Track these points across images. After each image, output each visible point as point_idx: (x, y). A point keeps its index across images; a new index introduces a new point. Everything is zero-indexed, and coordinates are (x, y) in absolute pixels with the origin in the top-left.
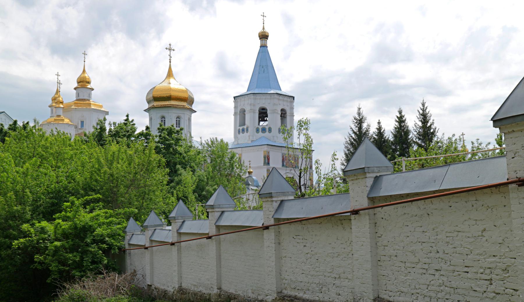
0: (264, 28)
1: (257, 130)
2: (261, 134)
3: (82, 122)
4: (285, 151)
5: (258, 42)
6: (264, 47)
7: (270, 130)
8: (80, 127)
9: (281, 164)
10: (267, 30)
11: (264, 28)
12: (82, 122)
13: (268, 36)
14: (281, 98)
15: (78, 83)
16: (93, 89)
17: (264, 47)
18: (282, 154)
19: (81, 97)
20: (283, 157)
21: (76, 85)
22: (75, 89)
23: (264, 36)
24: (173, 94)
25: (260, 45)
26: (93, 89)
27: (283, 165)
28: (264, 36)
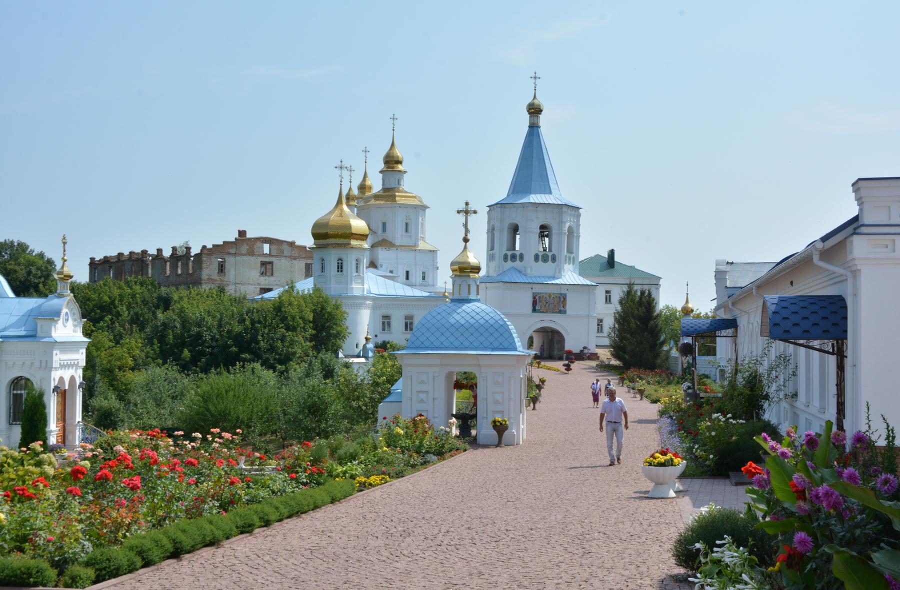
0: (535, 97)
1: (505, 258)
2: (510, 263)
3: (384, 224)
4: (537, 289)
6: (534, 128)
7: (522, 257)
10: (541, 101)
11: (535, 97)
12: (384, 224)
13: (541, 111)
16: (405, 172)
17: (534, 128)
18: (533, 293)
19: (388, 186)
20: (534, 298)
21: (381, 166)
22: (381, 172)
23: (534, 110)
24: (331, 232)
25: (528, 124)
26: (405, 172)
27: (534, 310)
28: (534, 110)
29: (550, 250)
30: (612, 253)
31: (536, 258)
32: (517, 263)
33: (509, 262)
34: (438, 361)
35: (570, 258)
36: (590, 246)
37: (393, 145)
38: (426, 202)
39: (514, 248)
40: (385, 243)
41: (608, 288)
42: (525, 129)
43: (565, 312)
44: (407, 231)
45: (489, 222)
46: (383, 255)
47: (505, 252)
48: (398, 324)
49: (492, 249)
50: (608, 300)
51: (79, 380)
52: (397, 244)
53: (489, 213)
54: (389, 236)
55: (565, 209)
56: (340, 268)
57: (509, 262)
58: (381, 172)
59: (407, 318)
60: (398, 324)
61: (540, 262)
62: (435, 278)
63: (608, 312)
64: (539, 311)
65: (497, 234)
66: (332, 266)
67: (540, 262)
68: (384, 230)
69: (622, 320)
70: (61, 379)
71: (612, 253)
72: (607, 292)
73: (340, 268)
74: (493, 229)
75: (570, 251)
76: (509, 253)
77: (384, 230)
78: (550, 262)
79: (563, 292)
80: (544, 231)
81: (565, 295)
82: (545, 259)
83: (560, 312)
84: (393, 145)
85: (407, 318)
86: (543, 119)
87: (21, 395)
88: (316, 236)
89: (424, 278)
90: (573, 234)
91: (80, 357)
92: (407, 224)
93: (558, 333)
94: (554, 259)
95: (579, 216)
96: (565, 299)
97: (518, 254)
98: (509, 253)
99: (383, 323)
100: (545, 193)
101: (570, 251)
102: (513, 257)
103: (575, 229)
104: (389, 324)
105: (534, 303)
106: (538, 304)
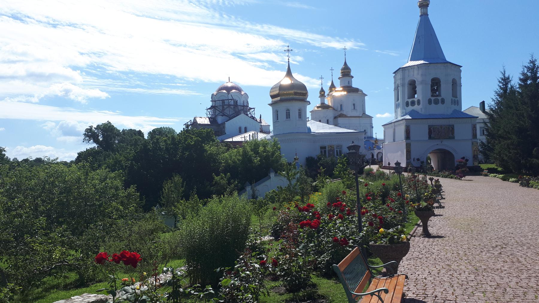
1: (407, 104)
2: (410, 108)
3: (341, 105)
5: (418, 12)
8: (339, 109)
12: (341, 105)
16: (353, 77)
17: (424, 16)
18: (429, 126)
20: (430, 129)
21: (340, 75)
22: (339, 78)
26: (353, 77)
27: (430, 138)
29: (439, 95)
31: (430, 102)
32: (416, 107)
33: (410, 106)
35: (455, 102)
37: (345, 63)
40: (341, 116)
42: (417, 19)
43: (453, 138)
45: (395, 83)
47: (406, 100)
49: (398, 100)
54: (344, 113)
56: (288, 116)
57: (410, 106)
58: (339, 78)
61: (433, 104)
62: (372, 132)
64: (434, 139)
65: (400, 89)
66: (282, 115)
67: (433, 104)
73: (288, 116)
74: (398, 87)
76: (410, 100)
78: (440, 104)
80: (435, 84)
81: (453, 126)
82: (436, 102)
84: (345, 63)
86: (430, 10)
88: (273, 97)
90: (456, 85)
94: (443, 101)
95: (461, 71)
97: (416, 100)
98: (410, 100)
99: (321, 152)
102: (413, 103)
103: (457, 80)
105: (430, 132)
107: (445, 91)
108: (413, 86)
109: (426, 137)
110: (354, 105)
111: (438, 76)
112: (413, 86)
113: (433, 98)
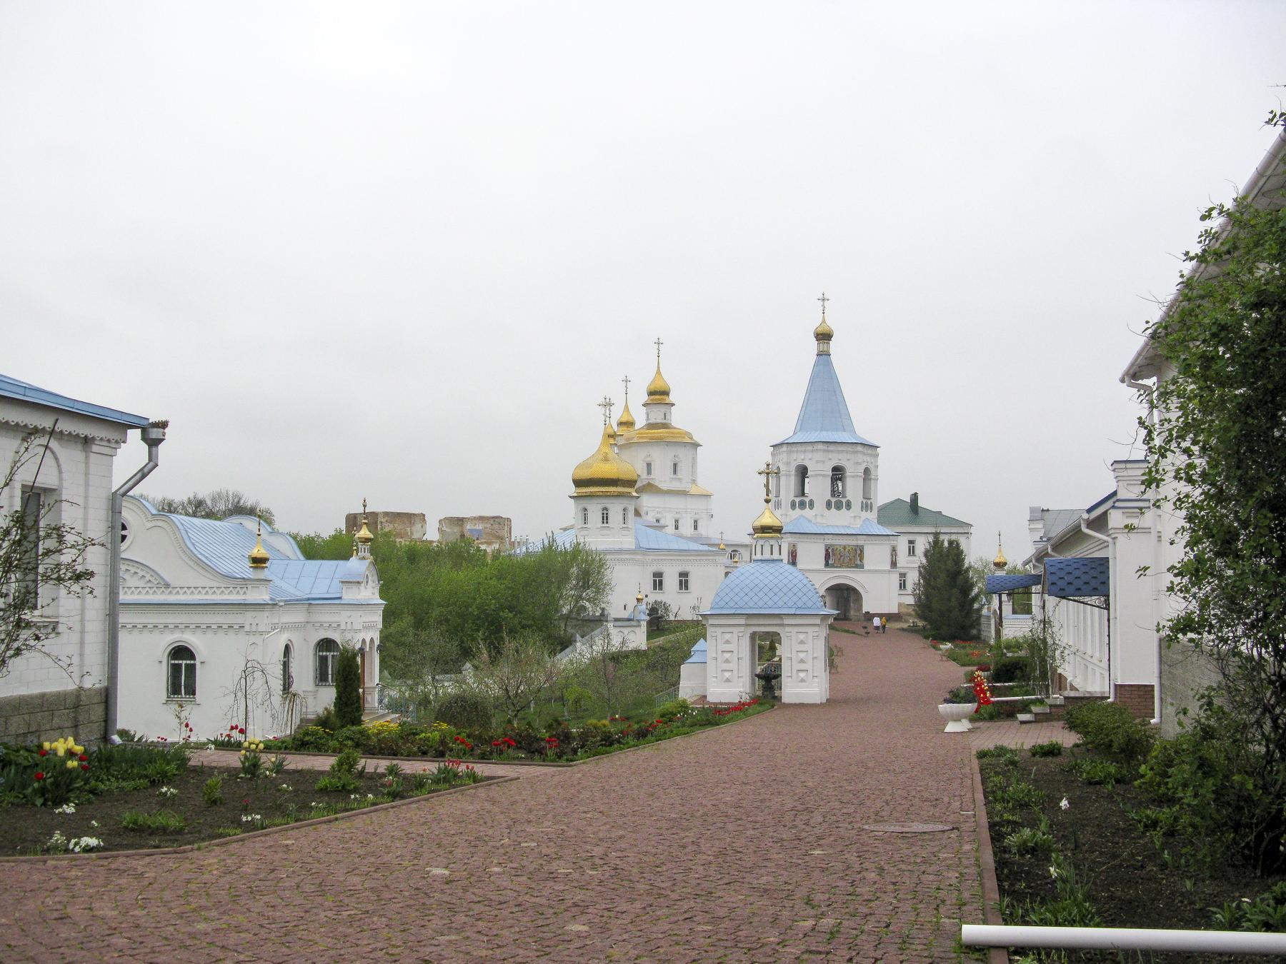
1: (793, 505)
3: (649, 465)
4: (830, 541)
6: (823, 355)
7: (812, 504)
9: (823, 562)
10: (833, 324)
12: (649, 465)
14: (832, 448)
15: (651, 393)
17: (823, 355)
19: (652, 421)
21: (645, 398)
23: (824, 337)
27: (827, 565)
28: (824, 337)
29: (844, 497)
30: (915, 497)
31: (829, 505)
34: (742, 621)
36: (889, 490)
37: (658, 372)
38: (697, 438)
39: (803, 494)
40: (650, 488)
41: (911, 537)
44: (675, 472)
46: (647, 502)
48: (671, 581)
50: (912, 552)
51: (377, 642)
52: (664, 486)
53: (773, 455)
55: (860, 448)
56: (605, 518)
59: (681, 575)
60: (671, 581)
63: (912, 565)
64: (833, 566)
68: (649, 472)
69: (928, 574)
70: (364, 641)
71: (915, 497)
72: (911, 542)
73: (605, 518)
75: (866, 496)
76: (797, 500)
77: (649, 472)
79: (860, 543)
83: (857, 566)
84: (658, 372)
85: (681, 575)
87: (326, 657)
89: (696, 528)
91: (377, 618)
92: (675, 465)
93: (854, 590)
94: (849, 506)
96: (862, 551)
97: (807, 500)
98: (797, 500)
100: (837, 430)
101: (866, 496)
102: (802, 505)
104: (661, 582)
106: (832, 557)
107: (853, 488)
108: (803, 472)
109: (821, 565)
110: (675, 465)
111: (843, 463)
112: (803, 472)
113: (833, 500)
